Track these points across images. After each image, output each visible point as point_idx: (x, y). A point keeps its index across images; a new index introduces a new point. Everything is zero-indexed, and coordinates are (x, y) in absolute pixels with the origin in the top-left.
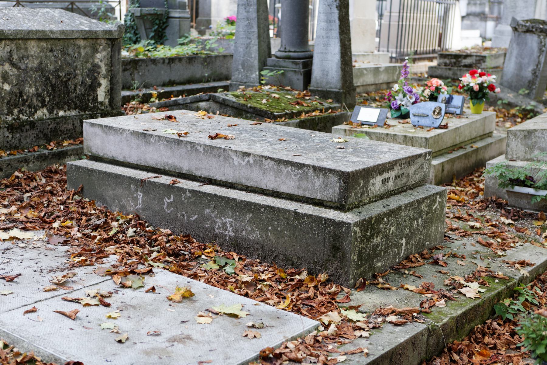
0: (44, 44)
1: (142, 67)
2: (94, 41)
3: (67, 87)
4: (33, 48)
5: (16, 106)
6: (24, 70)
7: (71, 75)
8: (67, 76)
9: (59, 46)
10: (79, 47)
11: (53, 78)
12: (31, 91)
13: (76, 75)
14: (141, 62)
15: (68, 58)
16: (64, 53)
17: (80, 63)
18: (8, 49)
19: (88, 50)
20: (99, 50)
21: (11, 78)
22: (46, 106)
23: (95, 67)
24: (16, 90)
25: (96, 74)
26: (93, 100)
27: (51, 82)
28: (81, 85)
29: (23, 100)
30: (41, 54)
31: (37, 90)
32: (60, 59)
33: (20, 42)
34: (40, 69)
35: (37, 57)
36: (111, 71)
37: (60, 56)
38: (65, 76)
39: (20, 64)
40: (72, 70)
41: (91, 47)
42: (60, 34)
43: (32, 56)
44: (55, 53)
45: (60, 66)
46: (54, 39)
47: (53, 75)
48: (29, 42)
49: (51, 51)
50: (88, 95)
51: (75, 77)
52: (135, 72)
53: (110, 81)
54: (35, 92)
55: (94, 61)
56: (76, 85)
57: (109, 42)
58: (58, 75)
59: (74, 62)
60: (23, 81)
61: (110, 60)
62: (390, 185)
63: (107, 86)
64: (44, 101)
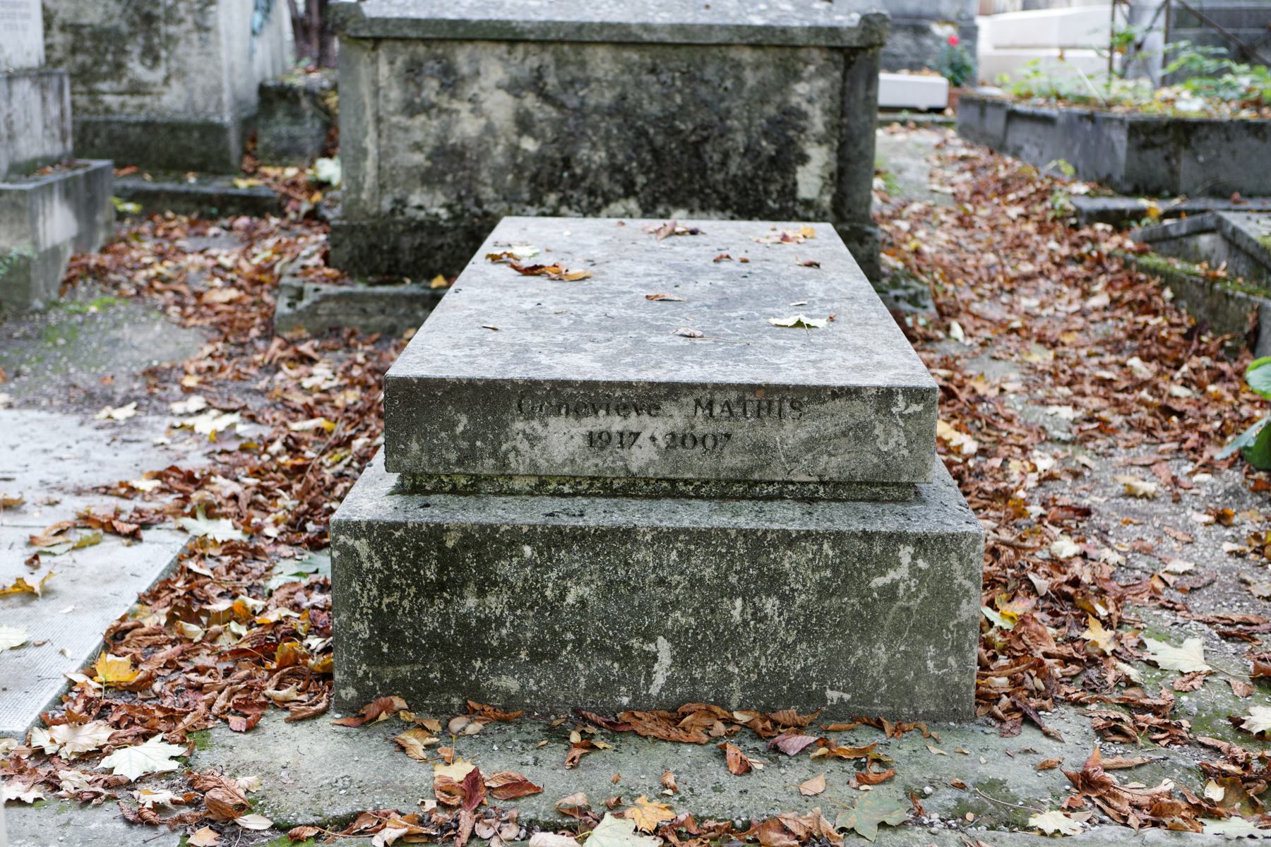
0: (633, 56)
1: (1209, 143)
2: (788, 52)
3: (698, 156)
4: (602, 62)
5: (552, 187)
6: (575, 110)
7: (713, 131)
8: (699, 132)
9: (679, 60)
10: (738, 66)
11: (656, 133)
12: (596, 158)
13: (730, 130)
14: (1206, 130)
15: (703, 91)
16: (689, 77)
17: (740, 102)
18: (533, 62)
19: (769, 73)
20: (805, 75)
21: (539, 126)
22: (635, 194)
23: (791, 118)
24: (552, 152)
25: (791, 133)
26: (782, 193)
27: (651, 142)
28: (744, 155)
29: (573, 176)
30: (626, 78)
31: (612, 156)
32: (680, 91)
33: (566, 48)
34: (621, 109)
35: (612, 85)
36: (840, 127)
37: (678, 83)
38: (694, 130)
39: (563, 98)
40: (715, 118)
41: (777, 67)
42: (671, 33)
43: (598, 80)
44: (663, 77)
45: (681, 107)
46: (652, 44)
47: (655, 126)
48: (589, 50)
49: (653, 71)
50: (766, 181)
51: (722, 136)
52: (1184, 153)
53: (838, 151)
54: (606, 162)
55: (785, 101)
56: (726, 155)
57: (837, 57)
58: (672, 127)
59: (722, 100)
60: (570, 134)
61: (838, 99)
62: (641, 457)
63: (827, 164)
64: (633, 184)
